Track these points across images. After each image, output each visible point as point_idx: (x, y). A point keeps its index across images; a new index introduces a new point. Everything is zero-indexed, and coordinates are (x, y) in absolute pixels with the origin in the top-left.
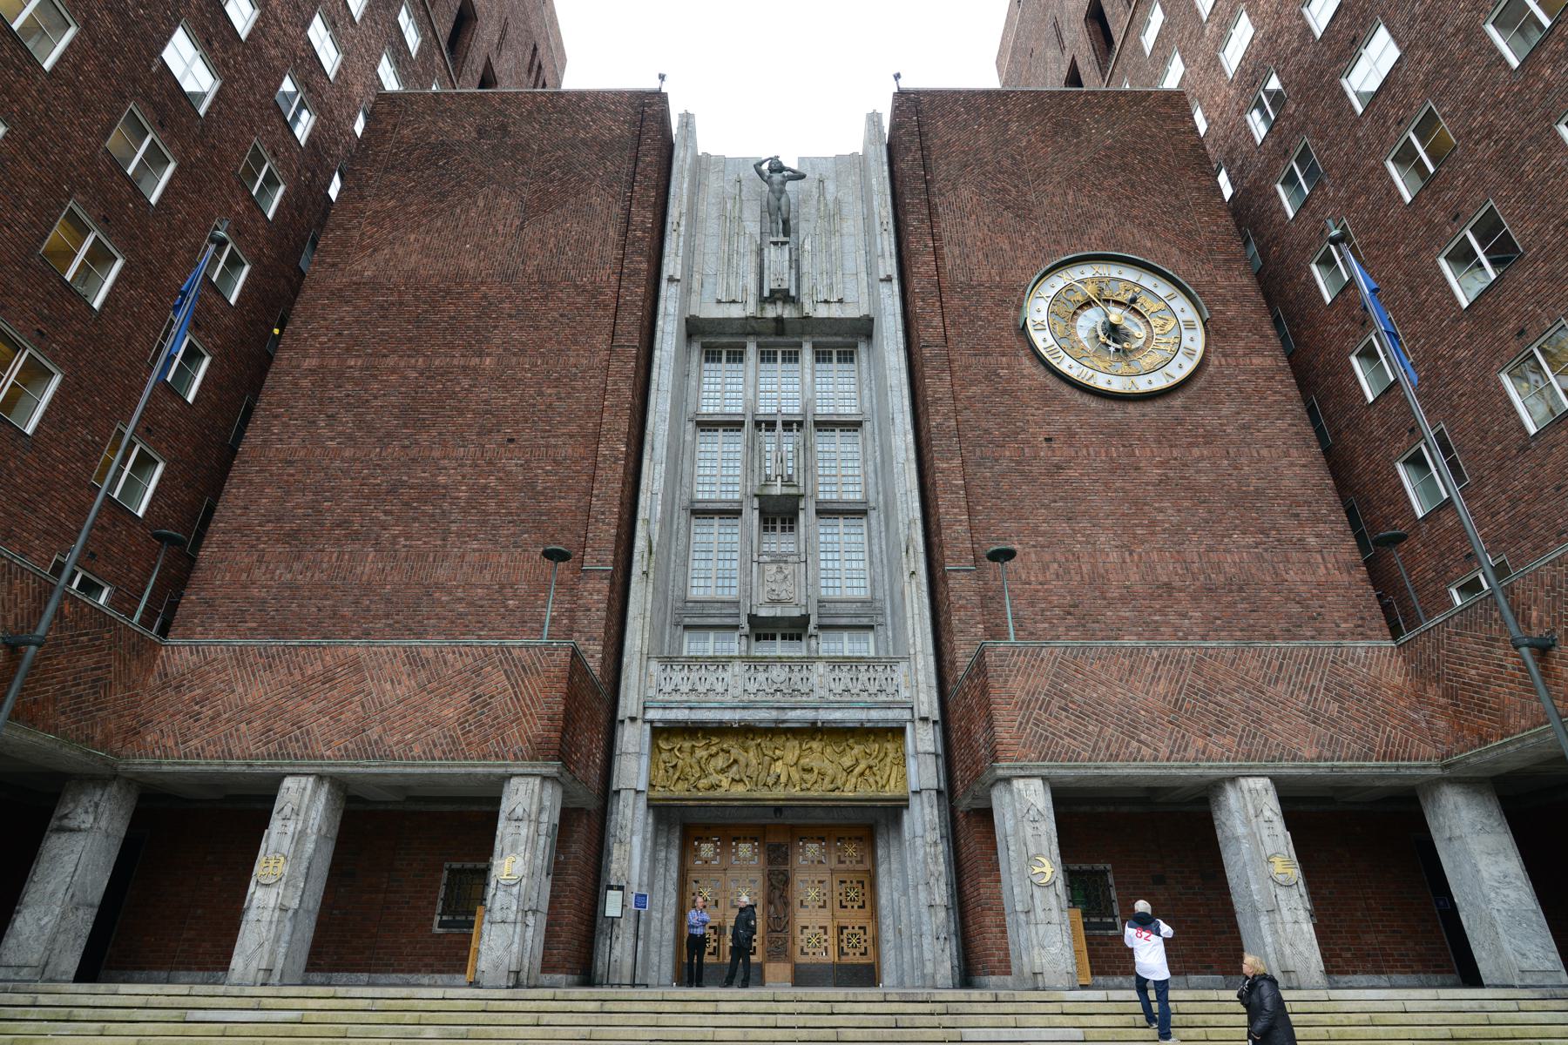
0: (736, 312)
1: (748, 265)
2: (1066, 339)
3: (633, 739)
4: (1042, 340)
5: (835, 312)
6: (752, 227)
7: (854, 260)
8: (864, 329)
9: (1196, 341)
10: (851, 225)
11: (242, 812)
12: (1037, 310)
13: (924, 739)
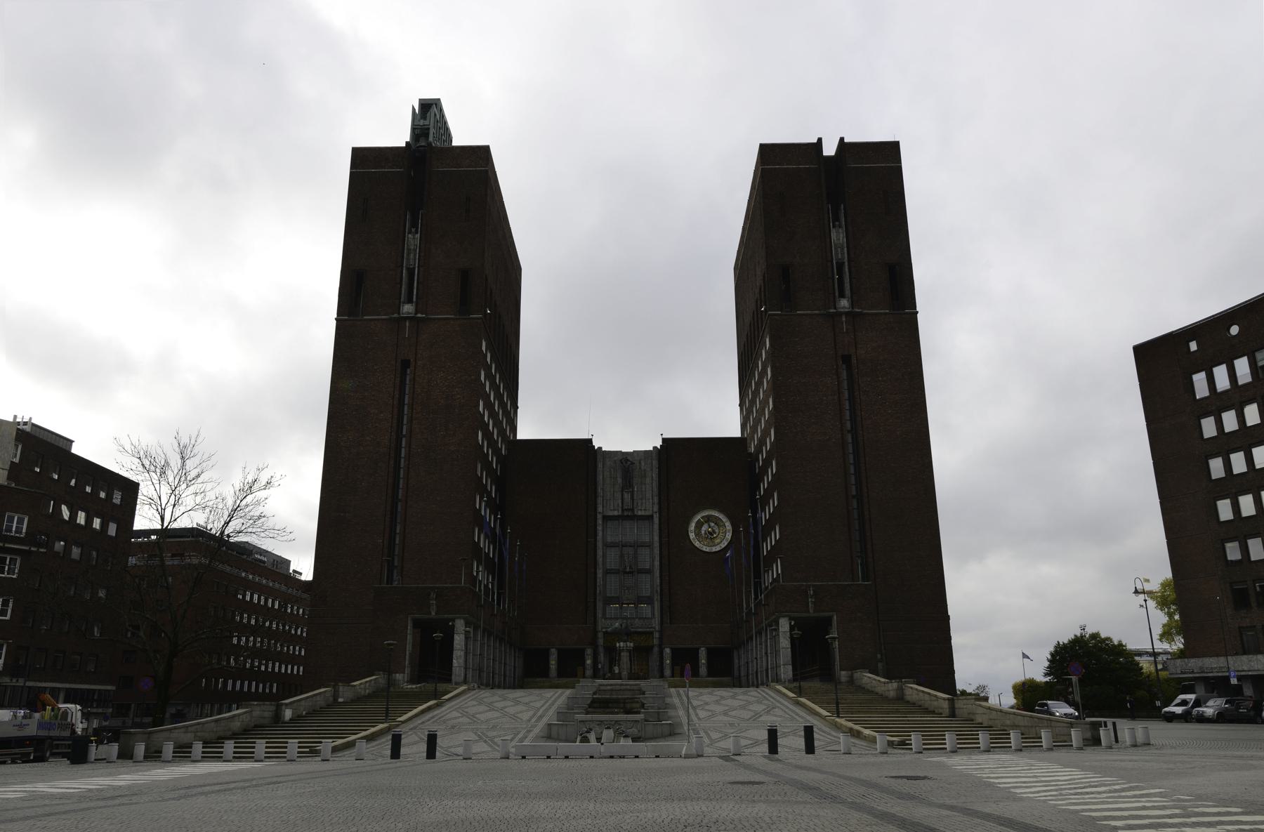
0: (616, 513)
1: (618, 495)
2: (698, 534)
3: (600, 635)
4: (692, 536)
5: (643, 513)
6: (620, 480)
7: (649, 495)
8: (650, 518)
9: (729, 536)
10: (648, 480)
11: (545, 655)
12: (692, 526)
13: (657, 635)
